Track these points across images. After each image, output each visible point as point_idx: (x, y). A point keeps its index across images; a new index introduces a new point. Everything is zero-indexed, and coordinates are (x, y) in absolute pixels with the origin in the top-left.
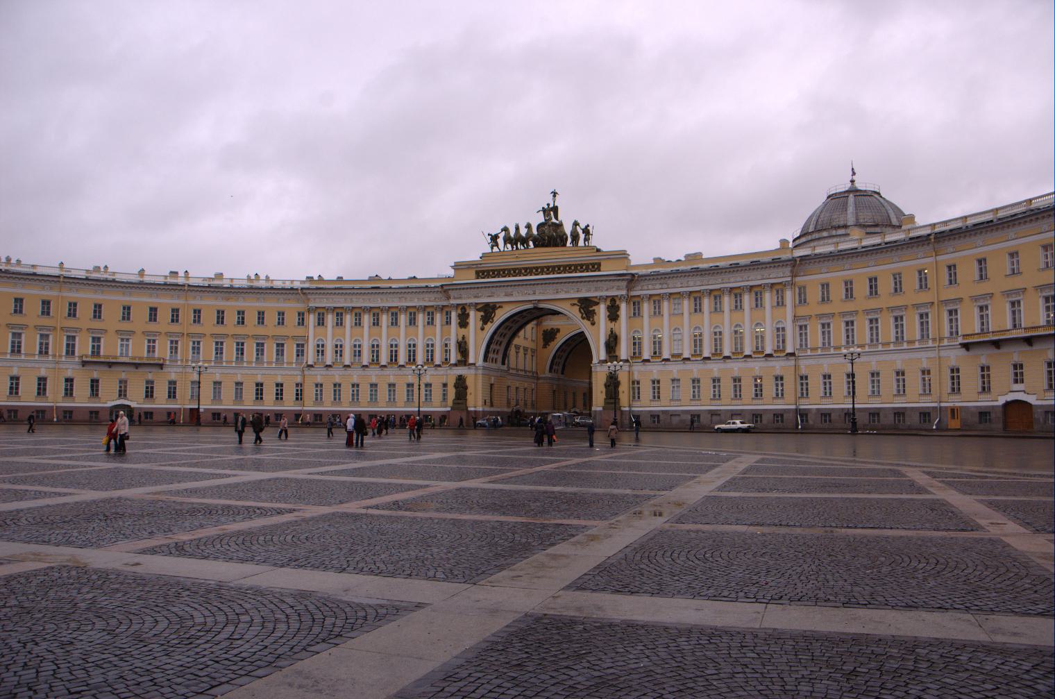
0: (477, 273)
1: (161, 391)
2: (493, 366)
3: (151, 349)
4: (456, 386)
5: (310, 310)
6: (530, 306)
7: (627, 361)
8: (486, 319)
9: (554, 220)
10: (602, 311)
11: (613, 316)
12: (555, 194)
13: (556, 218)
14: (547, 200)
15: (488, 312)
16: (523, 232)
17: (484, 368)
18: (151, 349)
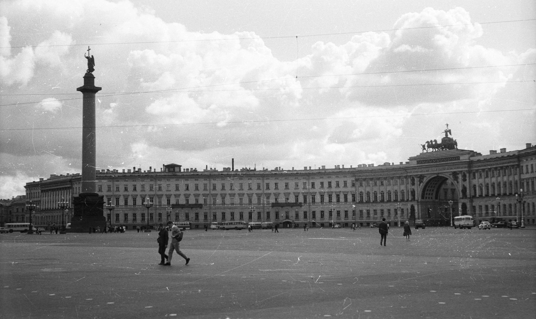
0: (417, 161)
1: (301, 215)
2: (430, 200)
3: (297, 200)
4: (411, 209)
5: (357, 180)
6: (436, 175)
7: (470, 198)
8: (421, 182)
9: (449, 136)
10: (460, 176)
11: (464, 180)
12: (447, 125)
13: (450, 134)
14: (445, 128)
15: (421, 177)
16: (434, 143)
17: (421, 202)
18: (297, 200)
